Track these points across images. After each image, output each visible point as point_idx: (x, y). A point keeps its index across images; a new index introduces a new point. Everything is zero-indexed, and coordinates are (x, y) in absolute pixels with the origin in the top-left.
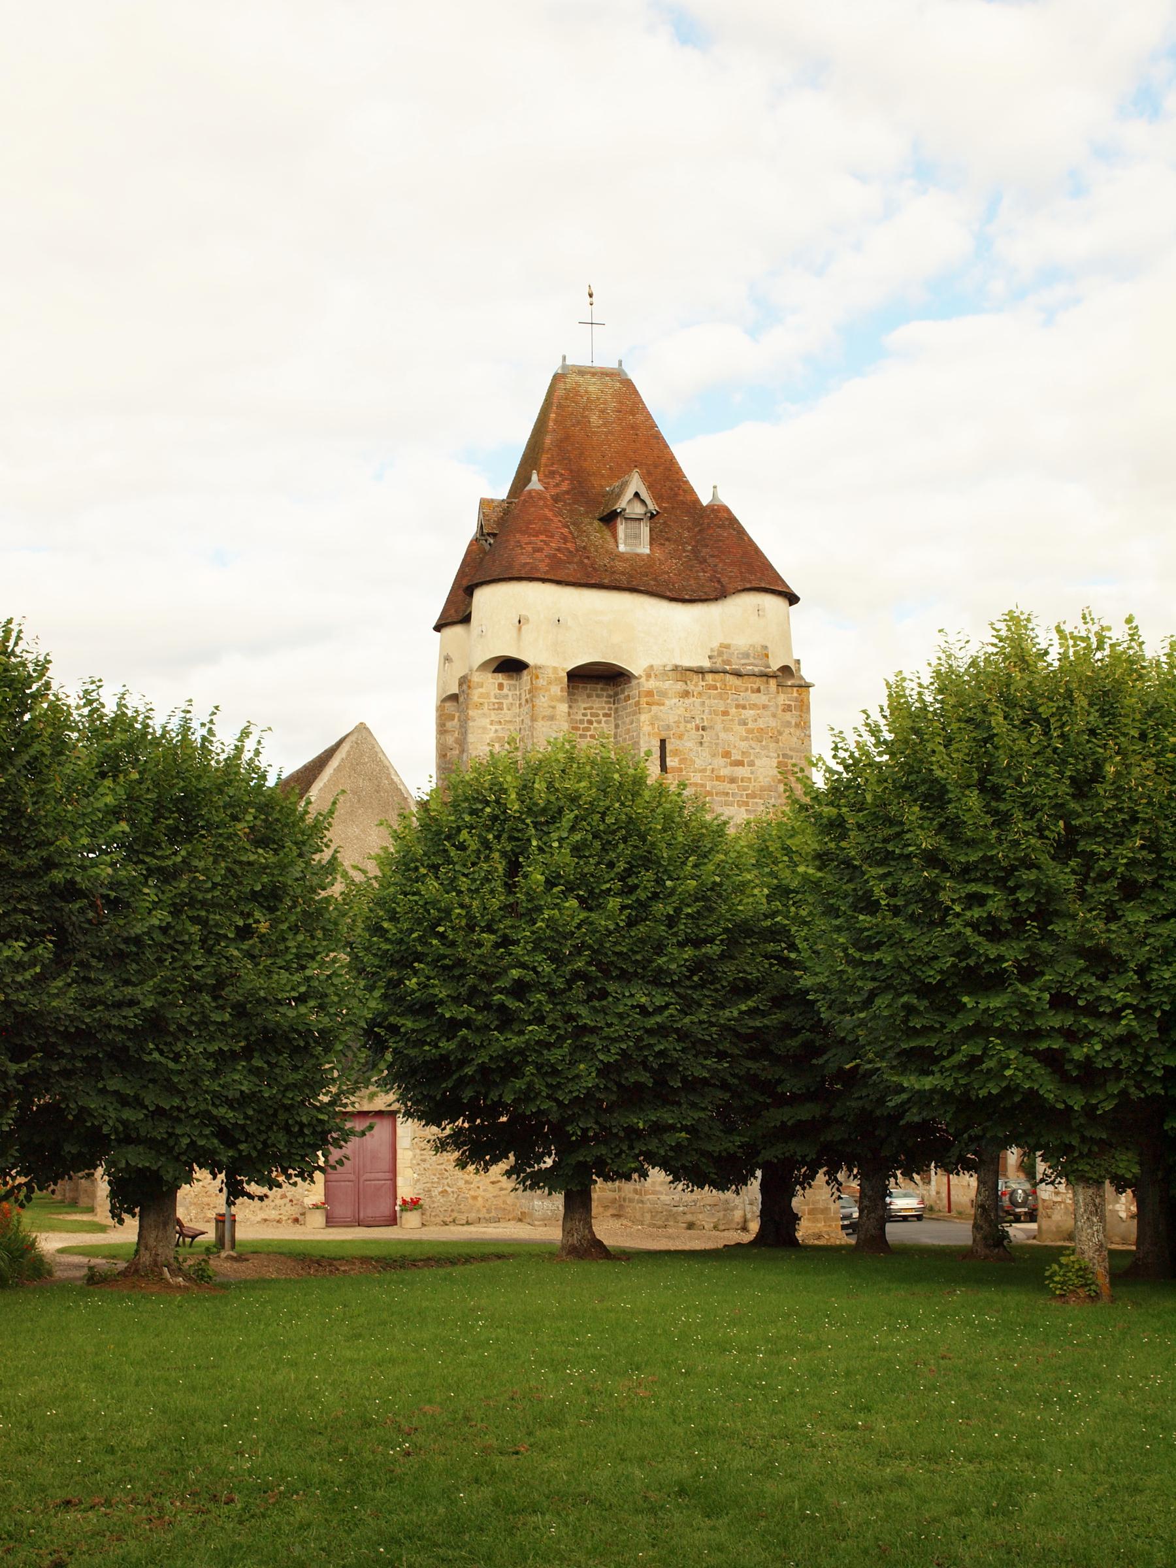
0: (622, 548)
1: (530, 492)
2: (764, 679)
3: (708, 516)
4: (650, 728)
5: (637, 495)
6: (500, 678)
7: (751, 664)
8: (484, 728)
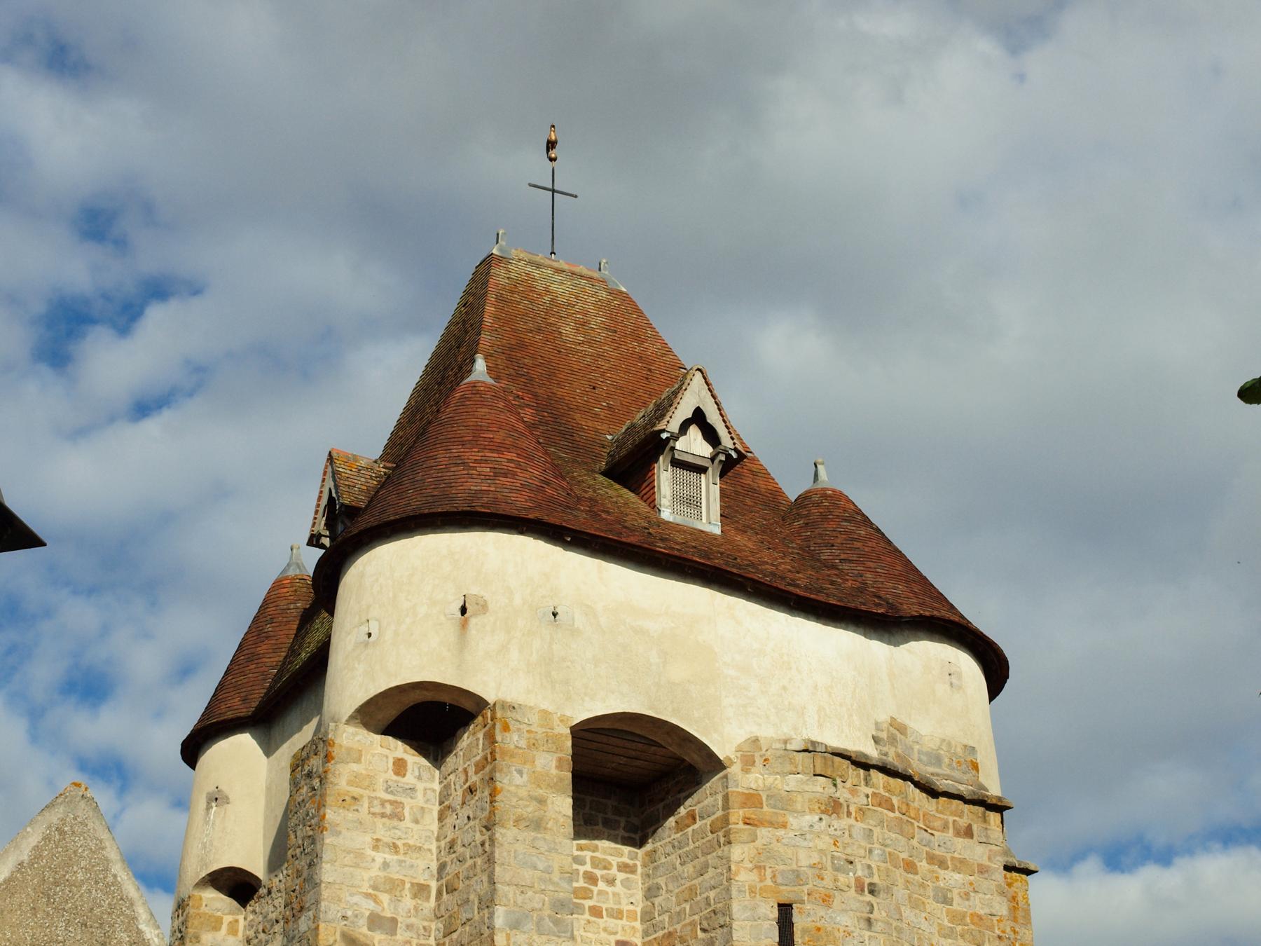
0: (666, 515)
1: (474, 385)
2: (981, 809)
3: (818, 505)
4: (754, 876)
5: (698, 418)
6: (398, 748)
7: (947, 777)
8: (359, 854)
